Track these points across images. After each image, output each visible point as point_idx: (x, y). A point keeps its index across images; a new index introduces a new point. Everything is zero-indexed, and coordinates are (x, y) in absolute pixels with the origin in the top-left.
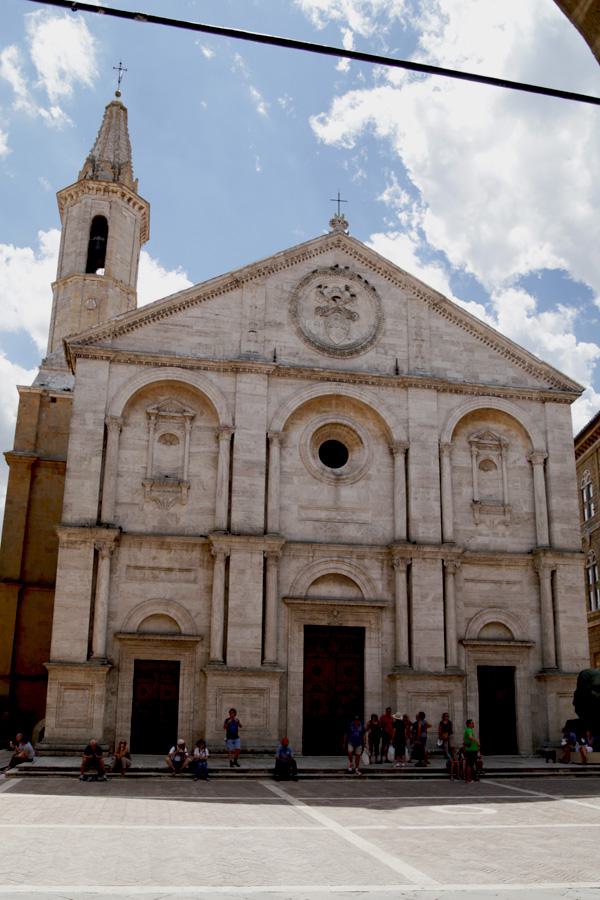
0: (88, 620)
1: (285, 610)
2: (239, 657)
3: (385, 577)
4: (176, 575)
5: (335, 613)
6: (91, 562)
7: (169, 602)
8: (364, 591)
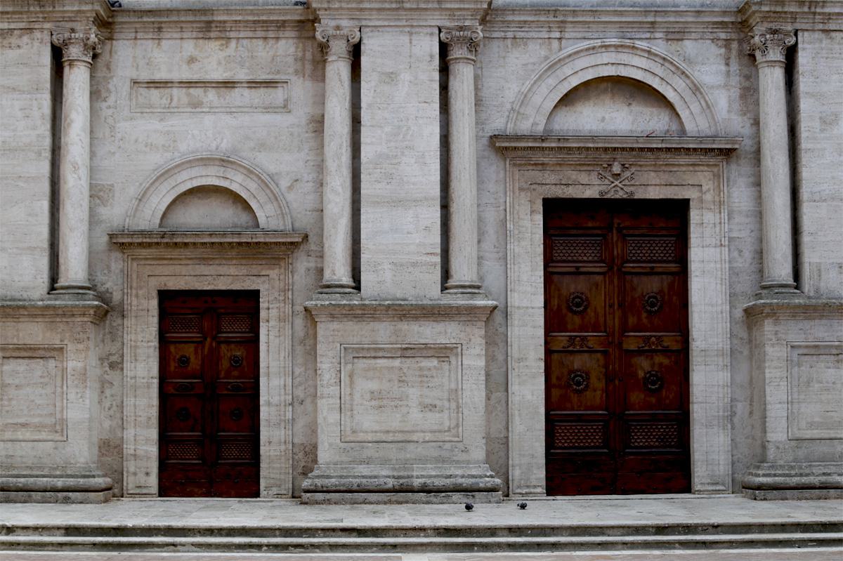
0: (45, 205)
1: (495, 169)
2: (388, 276)
3: (735, 80)
4: (241, 96)
5: (616, 168)
6: (46, 73)
7: (224, 162)
8: (684, 114)
